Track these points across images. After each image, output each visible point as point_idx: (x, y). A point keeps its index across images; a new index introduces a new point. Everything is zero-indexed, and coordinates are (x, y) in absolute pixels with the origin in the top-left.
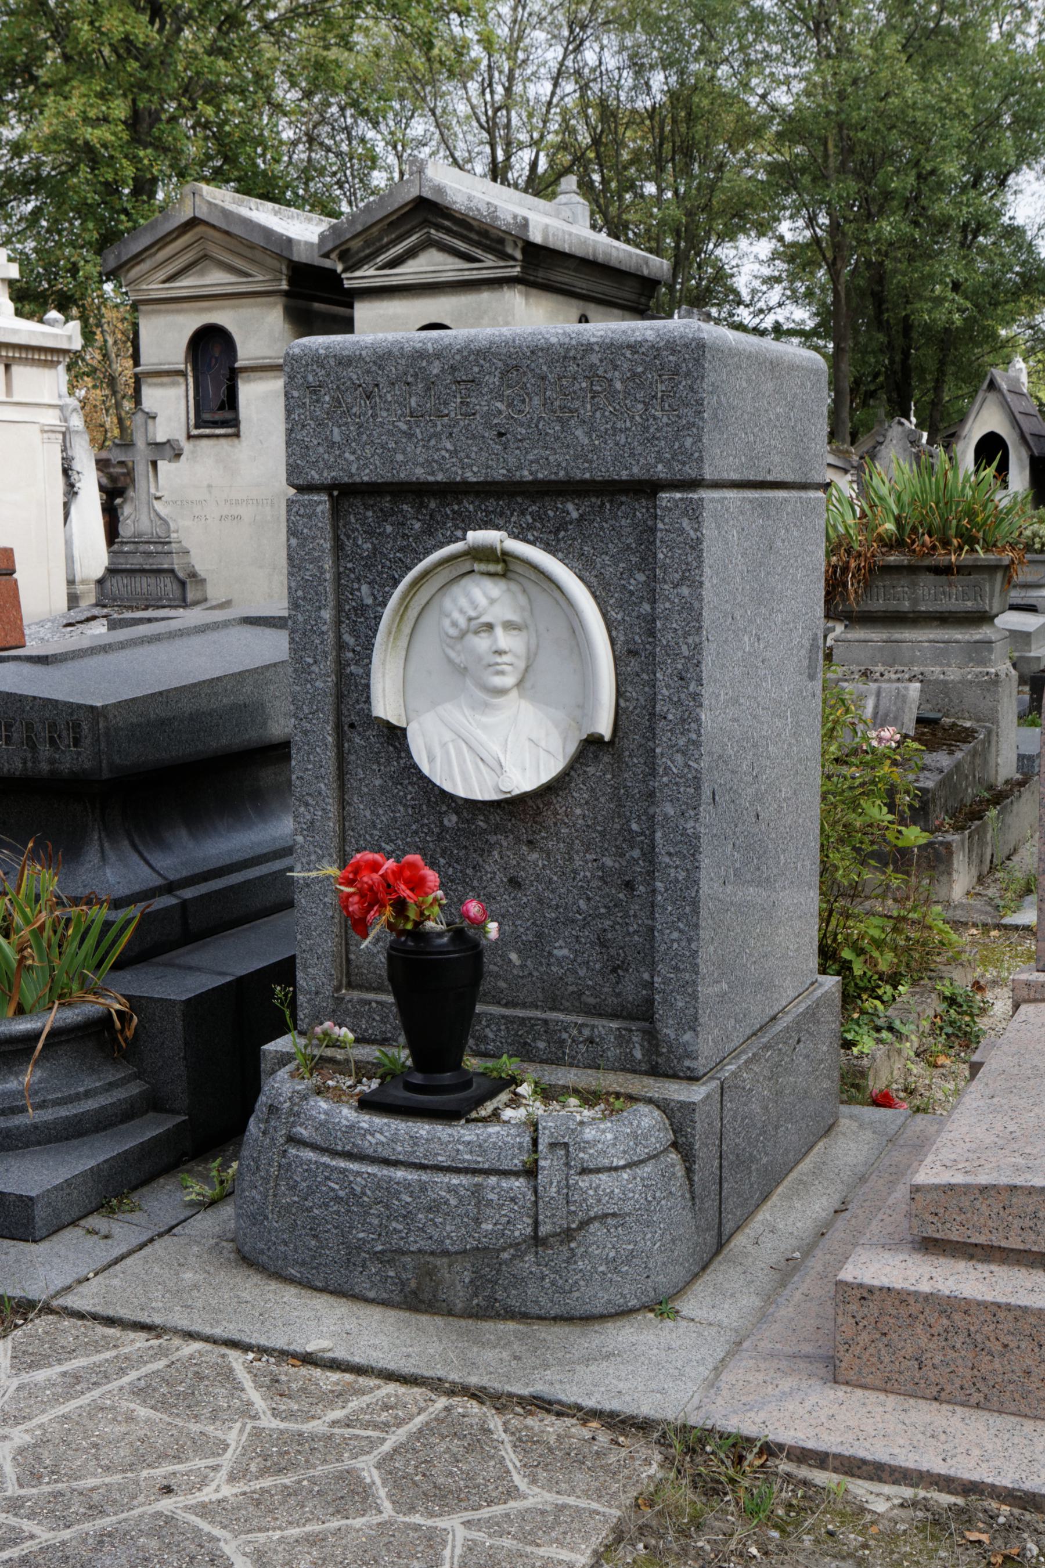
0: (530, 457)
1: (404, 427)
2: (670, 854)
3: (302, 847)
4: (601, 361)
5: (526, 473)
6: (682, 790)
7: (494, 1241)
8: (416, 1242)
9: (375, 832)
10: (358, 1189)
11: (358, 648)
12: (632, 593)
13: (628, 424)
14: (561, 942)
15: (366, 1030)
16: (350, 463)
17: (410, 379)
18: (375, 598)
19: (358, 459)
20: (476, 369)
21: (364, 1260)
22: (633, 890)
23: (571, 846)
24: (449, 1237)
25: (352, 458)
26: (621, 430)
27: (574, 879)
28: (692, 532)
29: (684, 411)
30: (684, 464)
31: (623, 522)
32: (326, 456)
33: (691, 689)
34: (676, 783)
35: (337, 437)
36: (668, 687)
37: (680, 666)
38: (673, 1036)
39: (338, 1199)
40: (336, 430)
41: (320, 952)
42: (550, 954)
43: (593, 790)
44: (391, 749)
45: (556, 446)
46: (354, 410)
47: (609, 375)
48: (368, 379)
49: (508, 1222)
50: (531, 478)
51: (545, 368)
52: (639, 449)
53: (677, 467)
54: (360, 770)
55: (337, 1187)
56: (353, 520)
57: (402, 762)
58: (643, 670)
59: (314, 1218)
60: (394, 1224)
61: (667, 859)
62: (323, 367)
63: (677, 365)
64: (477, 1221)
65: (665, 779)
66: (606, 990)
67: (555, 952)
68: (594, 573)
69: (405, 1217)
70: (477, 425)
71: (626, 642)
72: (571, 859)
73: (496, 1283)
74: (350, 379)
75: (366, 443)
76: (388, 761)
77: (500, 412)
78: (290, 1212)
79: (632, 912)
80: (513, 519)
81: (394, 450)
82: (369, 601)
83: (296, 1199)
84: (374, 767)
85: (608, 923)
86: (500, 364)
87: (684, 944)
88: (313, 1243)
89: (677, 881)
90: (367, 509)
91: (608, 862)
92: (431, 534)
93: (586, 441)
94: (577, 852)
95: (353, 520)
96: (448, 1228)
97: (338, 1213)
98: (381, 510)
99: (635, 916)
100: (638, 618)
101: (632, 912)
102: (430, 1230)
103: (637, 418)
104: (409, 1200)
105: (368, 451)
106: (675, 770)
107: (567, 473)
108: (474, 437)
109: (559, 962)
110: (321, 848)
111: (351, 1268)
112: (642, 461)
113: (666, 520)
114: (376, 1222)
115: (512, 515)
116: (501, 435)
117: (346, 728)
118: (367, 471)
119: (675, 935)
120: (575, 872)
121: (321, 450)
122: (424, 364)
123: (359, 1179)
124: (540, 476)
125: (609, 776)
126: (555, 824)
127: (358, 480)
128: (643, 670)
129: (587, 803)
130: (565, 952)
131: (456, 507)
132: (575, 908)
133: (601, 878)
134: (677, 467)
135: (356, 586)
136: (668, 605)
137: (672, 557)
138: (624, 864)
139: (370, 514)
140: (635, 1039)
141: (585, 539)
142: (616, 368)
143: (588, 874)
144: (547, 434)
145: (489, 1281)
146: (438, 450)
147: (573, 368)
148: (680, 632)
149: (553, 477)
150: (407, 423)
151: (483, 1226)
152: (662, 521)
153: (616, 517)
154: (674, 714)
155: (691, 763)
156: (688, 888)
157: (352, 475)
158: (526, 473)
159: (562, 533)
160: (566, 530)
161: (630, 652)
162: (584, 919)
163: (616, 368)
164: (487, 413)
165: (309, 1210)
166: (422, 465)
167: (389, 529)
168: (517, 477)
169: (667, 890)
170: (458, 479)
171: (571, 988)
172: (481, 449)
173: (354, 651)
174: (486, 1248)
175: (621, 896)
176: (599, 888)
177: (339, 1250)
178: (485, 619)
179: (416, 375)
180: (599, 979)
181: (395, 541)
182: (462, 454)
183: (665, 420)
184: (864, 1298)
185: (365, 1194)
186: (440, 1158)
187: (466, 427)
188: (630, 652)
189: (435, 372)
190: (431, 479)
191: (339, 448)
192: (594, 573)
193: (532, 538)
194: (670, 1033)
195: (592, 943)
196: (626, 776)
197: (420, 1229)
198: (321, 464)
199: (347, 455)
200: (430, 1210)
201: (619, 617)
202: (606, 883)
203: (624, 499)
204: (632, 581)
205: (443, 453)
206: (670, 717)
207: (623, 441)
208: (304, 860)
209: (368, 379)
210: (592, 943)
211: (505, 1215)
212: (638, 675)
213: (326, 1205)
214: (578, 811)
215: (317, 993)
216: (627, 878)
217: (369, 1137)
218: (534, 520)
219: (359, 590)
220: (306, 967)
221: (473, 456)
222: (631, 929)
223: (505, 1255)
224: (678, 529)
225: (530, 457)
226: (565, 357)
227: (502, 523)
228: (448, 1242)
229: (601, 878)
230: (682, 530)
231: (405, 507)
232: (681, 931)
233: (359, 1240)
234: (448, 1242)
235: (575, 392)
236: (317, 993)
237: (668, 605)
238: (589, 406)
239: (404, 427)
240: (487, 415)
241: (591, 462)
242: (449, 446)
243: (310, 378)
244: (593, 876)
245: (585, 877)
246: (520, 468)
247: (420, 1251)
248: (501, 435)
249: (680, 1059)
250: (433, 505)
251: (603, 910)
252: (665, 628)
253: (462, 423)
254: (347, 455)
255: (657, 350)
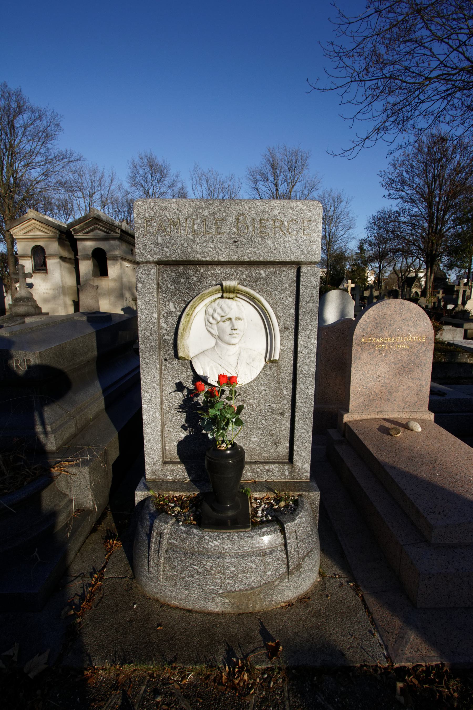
0: (248, 251)
1: (192, 237)
2: (302, 402)
3: (146, 409)
4: (279, 213)
5: (246, 258)
6: (307, 379)
7: (272, 578)
8: (238, 587)
9: (176, 401)
10: (208, 568)
11: (168, 329)
12: (286, 306)
13: (290, 239)
14: (254, 436)
15: (176, 476)
16: (166, 252)
17: (194, 217)
18: (176, 309)
19: (170, 250)
20: (224, 214)
21: (214, 597)
22: (284, 415)
23: (259, 401)
24: (253, 582)
25: (167, 250)
26: (287, 242)
27: (260, 413)
28: (314, 282)
29: (313, 235)
30: (312, 256)
31: (284, 278)
32: (155, 249)
33: (312, 342)
34: (305, 377)
35: (160, 240)
36: (303, 341)
37: (308, 333)
38: (300, 466)
39: (198, 573)
40: (159, 238)
41: (155, 448)
42: (250, 440)
43: (269, 380)
44: (183, 368)
45: (259, 247)
46: (168, 230)
47: (282, 219)
48: (175, 216)
49: (277, 569)
50: (248, 260)
51: (255, 215)
52: (294, 249)
53: (309, 256)
54: (169, 377)
55: (197, 568)
56: (166, 276)
57: (188, 373)
58: (290, 335)
59: (186, 582)
60: (228, 581)
61: (300, 404)
62: (153, 210)
63: (310, 216)
64: (265, 572)
65: (301, 375)
66: (272, 451)
67: (252, 439)
68: (271, 298)
69: (232, 577)
70: (225, 237)
71: (284, 324)
72: (259, 406)
73: (273, 594)
74: (166, 216)
75: (174, 244)
76: (182, 373)
77: (235, 232)
78: (173, 579)
79: (283, 423)
80: (238, 277)
81: (187, 247)
82: (173, 310)
83: (175, 573)
84: (176, 375)
85: (273, 428)
86: (235, 213)
87: (306, 434)
88: (186, 592)
89: (304, 412)
90: (172, 272)
91: (274, 406)
92: (201, 283)
93: (272, 246)
94: (262, 403)
95: (166, 276)
96: (253, 578)
97: (199, 579)
98: (179, 272)
99: (284, 424)
100: (289, 315)
101: (283, 423)
102: (245, 581)
103: (294, 237)
104: (234, 569)
105: (175, 247)
106: (305, 372)
107: (264, 258)
108: (223, 243)
109: (254, 443)
110: (155, 409)
111: (207, 600)
112: (295, 254)
113: (304, 277)
114: (219, 581)
115: (237, 275)
116: (235, 242)
117: (163, 361)
118: (174, 256)
119: (303, 431)
120: (261, 410)
121: (152, 246)
122: (201, 211)
123: (208, 563)
124: (252, 259)
125: (275, 375)
126: (253, 393)
127: (170, 259)
128: (290, 335)
129: (266, 385)
130: (256, 439)
131: (212, 272)
132: (260, 423)
133: (271, 412)
134: (309, 256)
135: (167, 303)
136: (304, 310)
137: (306, 292)
138: (280, 406)
139: (173, 274)
140: (286, 468)
141: (268, 285)
142: (285, 216)
143: (266, 411)
144: (255, 242)
145: (270, 594)
146: (207, 247)
147: (267, 216)
148: (308, 320)
149: (258, 260)
150: (193, 235)
151: (268, 574)
152: (303, 278)
153: (281, 276)
154: (305, 351)
155: (311, 369)
156: (308, 414)
157: (168, 257)
158: (246, 258)
159: (258, 282)
160: (260, 281)
161: (285, 328)
162: (264, 427)
163: (285, 216)
164: (229, 232)
165: (184, 578)
166: (200, 254)
167: (182, 280)
168: (242, 260)
169: (300, 415)
170: (216, 260)
171: (258, 452)
172: (226, 247)
173: (166, 330)
174: (269, 582)
175: (279, 418)
176: (270, 416)
177: (200, 594)
178: (228, 316)
179: (197, 216)
180: (269, 448)
181: (185, 285)
182: (218, 249)
183: (305, 238)
184: (430, 578)
185: (212, 570)
186: (245, 548)
187: (220, 238)
188: (285, 328)
189: (206, 214)
190: (204, 259)
191: (161, 246)
192: (271, 298)
193: (245, 284)
194: (299, 465)
195: (267, 435)
196: (282, 374)
197: (240, 581)
198: (153, 252)
199: (165, 249)
200: (244, 572)
201: (281, 315)
202: (273, 414)
203: (284, 269)
204: (287, 301)
205: (209, 249)
206: (303, 352)
207: (287, 246)
208: (147, 414)
209: (175, 216)
210: (267, 435)
211: (276, 567)
212: (288, 337)
213: (193, 576)
214: (263, 388)
215: (154, 464)
216: (281, 411)
217: (210, 543)
218: (247, 277)
219: (169, 305)
220: (149, 455)
221: (223, 250)
222: (282, 429)
223: (277, 583)
224: (309, 281)
225: (248, 251)
226: (264, 211)
227: (233, 278)
228: (253, 584)
229: (271, 412)
230: (311, 281)
231: (189, 271)
232: (305, 429)
233: (210, 589)
234: (253, 584)
235: (268, 226)
236: (154, 464)
237: (304, 310)
238: (273, 231)
239: (192, 237)
240: (229, 234)
241: (274, 254)
242: (212, 246)
243: (147, 215)
244: (268, 411)
245: (265, 412)
246: (243, 255)
247: (241, 590)
248: (235, 242)
249: (303, 473)
250: (202, 270)
251: (271, 423)
252: (303, 319)
253: (218, 237)
254: (165, 249)
255: (303, 210)
